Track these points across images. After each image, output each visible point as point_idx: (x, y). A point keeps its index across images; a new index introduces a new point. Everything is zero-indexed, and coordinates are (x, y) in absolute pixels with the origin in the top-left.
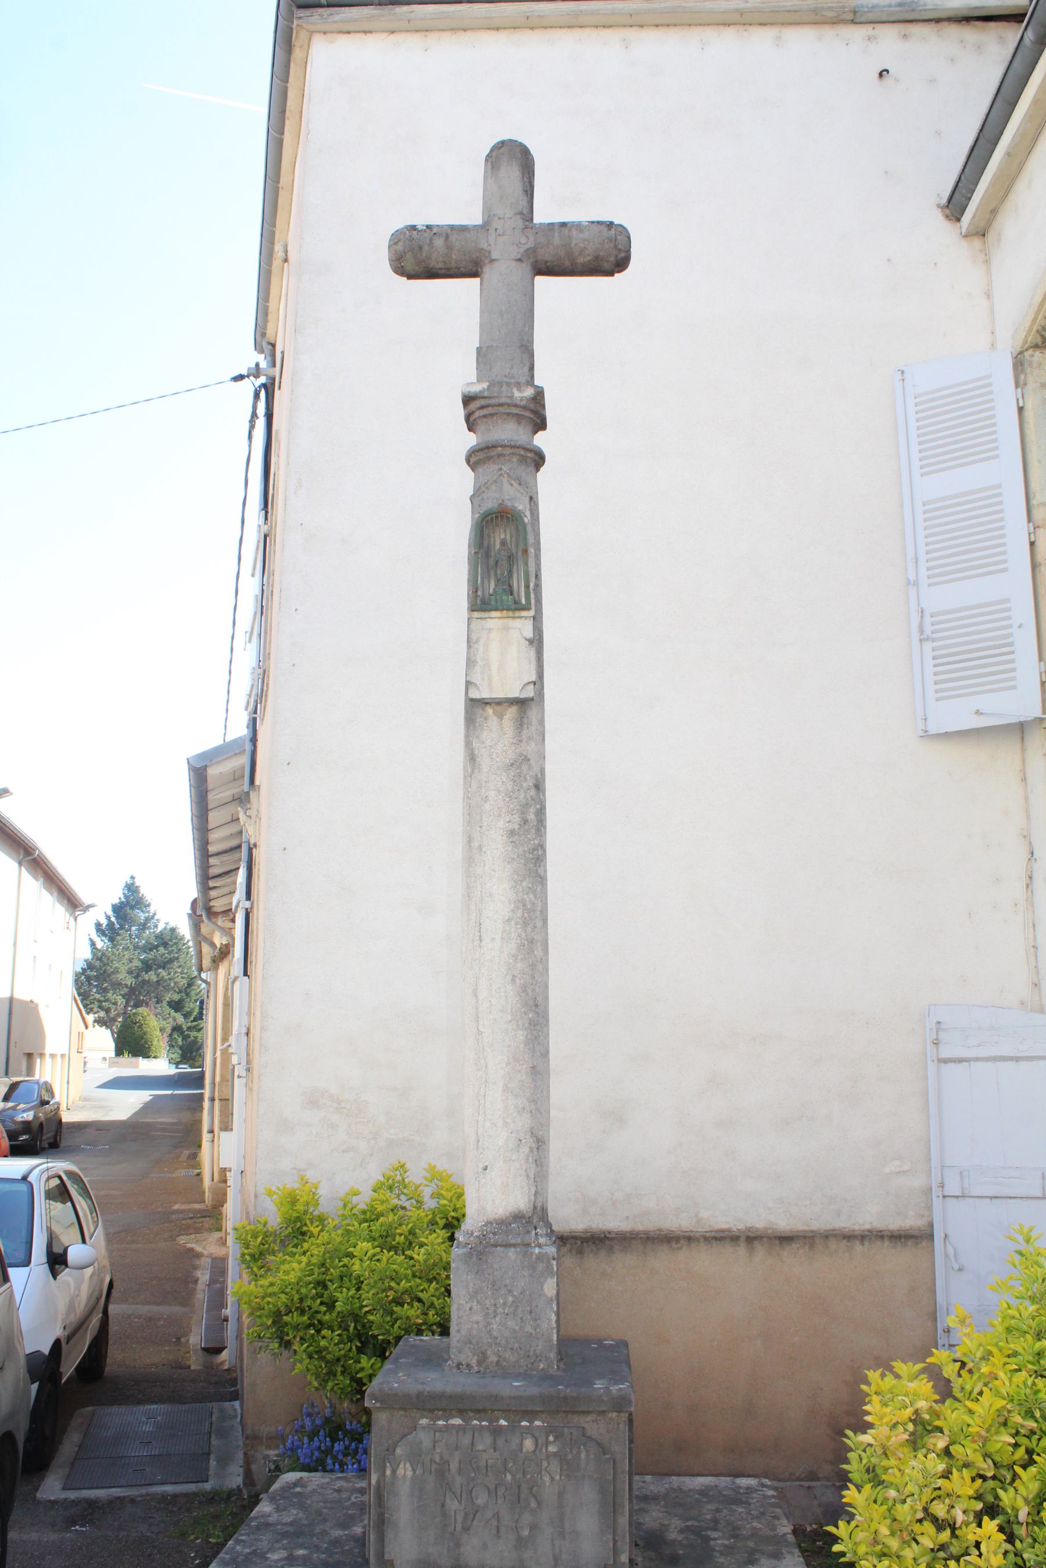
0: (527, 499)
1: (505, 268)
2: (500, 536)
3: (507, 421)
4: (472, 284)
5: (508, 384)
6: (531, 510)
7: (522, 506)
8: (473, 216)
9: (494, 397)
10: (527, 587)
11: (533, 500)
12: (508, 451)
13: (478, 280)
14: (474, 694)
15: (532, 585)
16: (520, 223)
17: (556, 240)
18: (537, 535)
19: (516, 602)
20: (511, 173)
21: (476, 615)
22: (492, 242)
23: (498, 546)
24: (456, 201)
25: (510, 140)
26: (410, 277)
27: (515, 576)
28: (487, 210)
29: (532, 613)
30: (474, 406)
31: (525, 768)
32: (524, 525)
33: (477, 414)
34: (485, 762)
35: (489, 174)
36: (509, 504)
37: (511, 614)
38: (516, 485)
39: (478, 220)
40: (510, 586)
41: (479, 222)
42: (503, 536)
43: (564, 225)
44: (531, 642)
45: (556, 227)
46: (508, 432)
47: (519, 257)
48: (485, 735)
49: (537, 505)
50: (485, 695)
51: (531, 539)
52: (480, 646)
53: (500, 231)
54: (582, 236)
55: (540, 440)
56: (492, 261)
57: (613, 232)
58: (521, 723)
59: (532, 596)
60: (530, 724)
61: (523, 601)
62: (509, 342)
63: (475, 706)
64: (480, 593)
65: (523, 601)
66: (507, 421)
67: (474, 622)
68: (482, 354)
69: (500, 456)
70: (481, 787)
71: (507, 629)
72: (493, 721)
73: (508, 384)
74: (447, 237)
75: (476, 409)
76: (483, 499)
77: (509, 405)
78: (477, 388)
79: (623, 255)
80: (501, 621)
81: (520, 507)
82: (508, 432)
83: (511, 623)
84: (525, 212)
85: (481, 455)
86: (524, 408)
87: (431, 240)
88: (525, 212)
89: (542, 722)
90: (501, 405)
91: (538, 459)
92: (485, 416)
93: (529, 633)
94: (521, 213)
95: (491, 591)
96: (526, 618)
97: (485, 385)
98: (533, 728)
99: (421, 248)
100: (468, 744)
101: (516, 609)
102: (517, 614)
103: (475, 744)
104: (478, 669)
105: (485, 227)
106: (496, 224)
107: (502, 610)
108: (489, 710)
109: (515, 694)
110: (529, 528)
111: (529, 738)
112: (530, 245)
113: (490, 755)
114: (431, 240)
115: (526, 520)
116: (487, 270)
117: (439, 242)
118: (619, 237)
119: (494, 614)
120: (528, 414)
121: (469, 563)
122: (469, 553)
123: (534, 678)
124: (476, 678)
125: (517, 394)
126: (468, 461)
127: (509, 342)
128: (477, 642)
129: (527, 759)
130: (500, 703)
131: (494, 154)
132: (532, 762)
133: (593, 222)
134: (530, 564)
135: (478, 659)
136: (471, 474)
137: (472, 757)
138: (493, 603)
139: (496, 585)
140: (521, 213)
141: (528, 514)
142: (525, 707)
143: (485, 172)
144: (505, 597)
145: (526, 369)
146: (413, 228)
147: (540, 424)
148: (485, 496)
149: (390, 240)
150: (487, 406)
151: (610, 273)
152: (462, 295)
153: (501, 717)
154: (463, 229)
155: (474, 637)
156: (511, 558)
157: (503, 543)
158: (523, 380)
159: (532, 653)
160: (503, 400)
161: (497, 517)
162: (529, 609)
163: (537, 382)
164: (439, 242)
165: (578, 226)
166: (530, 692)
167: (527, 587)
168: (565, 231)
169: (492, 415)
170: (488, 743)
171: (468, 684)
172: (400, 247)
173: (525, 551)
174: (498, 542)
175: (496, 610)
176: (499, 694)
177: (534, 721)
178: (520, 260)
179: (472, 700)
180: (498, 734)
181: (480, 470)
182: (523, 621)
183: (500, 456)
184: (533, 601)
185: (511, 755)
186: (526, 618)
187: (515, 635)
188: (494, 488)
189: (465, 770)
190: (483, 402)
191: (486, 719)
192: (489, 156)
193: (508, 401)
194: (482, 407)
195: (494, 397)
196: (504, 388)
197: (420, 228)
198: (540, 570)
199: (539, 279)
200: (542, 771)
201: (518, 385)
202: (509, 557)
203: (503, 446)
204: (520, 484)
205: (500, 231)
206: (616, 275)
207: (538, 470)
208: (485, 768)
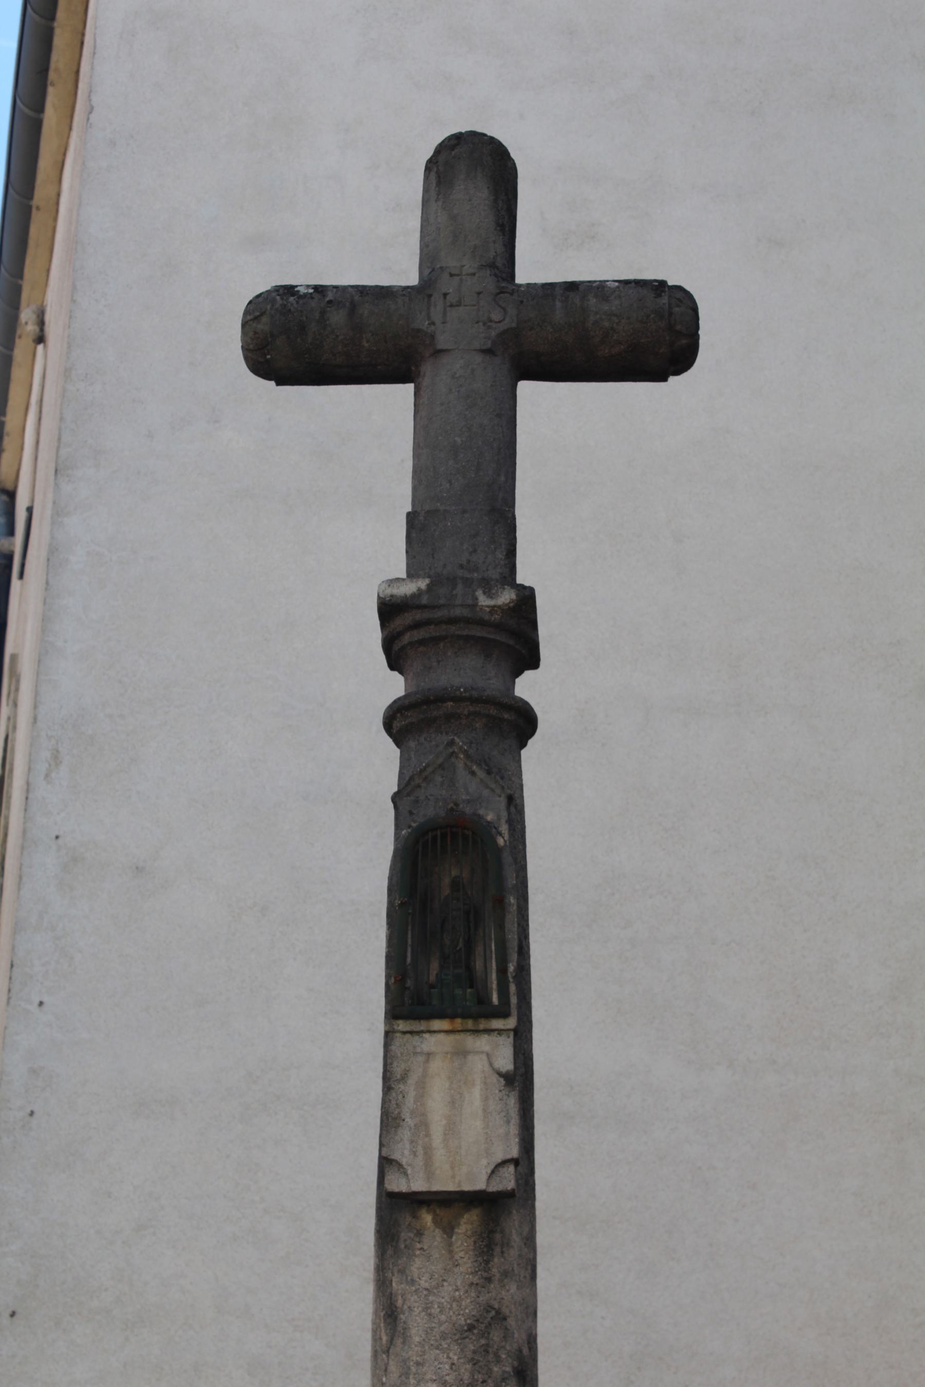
0: (503, 801)
1: (459, 367)
2: (449, 873)
3: (462, 648)
4: (402, 395)
5: (468, 582)
6: (510, 822)
7: (493, 813)
8: (401, 268)
13: (410, 387)
14: (397, 1184)
15: (511, 968)
16: (489, 283)
19: (482, 999)
20: (473, 195)
21: (401, 1025)
23: (446, 891)
24: (374, 242)
25: (473, 134)
27: (479, 949)
28: (429, 258)
29: (511, 1023)
30: (399, 623)
31: (496, 1335)
32: (499, 850)
33: (406, 638)
34: (416, 1324)
35: (433, 193)
36: (468, 810)
37: (470, 1024)
38: (481, 774)
40: (470, 969)
41: (413, 279)
42: (454, 873)
43: (572, 286)
44: (509, 1079)
46: (463, 672)
47: (489, 344)
48: (416, 1266)
49: (521, 812)
50: (419, 1185)
51: (511, 881)
53: (451, 299)
54: (606, 307)
55: (527, 687)
57: (665, 300)
58: (488, 1244)
59: (513, 988)
60: (506, 1244)
61: (495, 999)
62: (466, 505)
63: (398, 1211)
64: (409, 983)
65: (495, 999)
66: (462, 648)
67: (398, 1040)
68: (416, 524)
69: (450, 717)
70: (406, 1374)
71: (462, 1053)
72: (434, 1239)
73: (468, 582)
75: (404, 627)
76: (417, 801)
77: (468, 621)
78: (409, 589)
79: (684, 341)
80: (451, 1038)
81: (489, 818)
82: (463, 672)
83: (470, 1041)
84: (500, 262)
86: (498, 627)
87: (323, 313)
88: (500, 262)
89: (530, 1240)
91: (523, 723)
92: (422, 642)
93: (505, 1060)
94: (492, 266)
95: (432, 978)
96: (500, 1032)
97: (423, 584)
98: (513, 1253)
99: (303, 328)
100: (382, 1284)
101: (476, 1017)
102: (483, 1024)
103: (397, 1285)
104: (405, 1134)
105: (424, 290)
106: (448, 285)
107: (452, 1017)
108: (427, 1218)
109: (480, 1184)
110: (507, 858)
111: (505, 1274)
112: (509, 322)
113: (427, 1309)
114: (323, 313)
115: (501, 842)
116: (427, 369)
117: (337, 318)
118: (676, 310)
119: (437, 1024)
121: (390, 924)
122: (390, 904)
123: (514, 1152)
124: (402, 1152)
125: (484, 601)
126: (389, 724)
127: (466, 505)
128: (404, 1078)
129: (500, 1317)
130: (448, 1203)
131: (442, 158)
132: (511, 1322)
133: (627, 282)
135: (406, 1114)
136: (394, 752)
137: (389, 1313)
138: (435, 1002)
140: (492, 266)
141: (504, 829)
142: (499, 1213)
143: (426, 190)
144: (458, 992)
145: (500, 555)
146: (289, 290)
147: (529, 658)
149: (246, 313)
151: (660, 376)
152: (382, 415)
153: (449, 1230)
154: (382, 293)
155: (398, 1069)
157: (456, 884)
158: (494, 574)
159: (512, 1102)
160: (458, 612)
162: (505, 1015)
163: (523, 577)
164: (337, 318)
165: (598, 289)
166: (507, 1181)
167: (502, 971)
169: (435, 640)
170: (424, 1283)
171: (385, 1163)
172: (264, 326)
173: (500, 903)
174: (447, 881)
175: (441, 1016)
176: (444, 1184)
177: (516, 1240)
179: (392, 1195)
180: (442, 1267)
181: (412, 744)
182: (494, 1038)
183: (450, 717)
184: (514, 1000)
185: (468, 1307)
186: (500, 1032)
187: (478, 1065)
188: (439, 779)
189: (376, 1339)
190: (418, 616)
191: (420, 1234)
192: (431, 165)
193: (466, 612)
194: (416, 626)
197: (302, 290)
198: (526, 937)
199: (526, 389)
200: (532, 1340)
201: (488, 587)
203: (458, 699)
204: (489, 772)
205: (451, 299)
206: (672, 379)
207: (523, 745)
208: (416, 1335)
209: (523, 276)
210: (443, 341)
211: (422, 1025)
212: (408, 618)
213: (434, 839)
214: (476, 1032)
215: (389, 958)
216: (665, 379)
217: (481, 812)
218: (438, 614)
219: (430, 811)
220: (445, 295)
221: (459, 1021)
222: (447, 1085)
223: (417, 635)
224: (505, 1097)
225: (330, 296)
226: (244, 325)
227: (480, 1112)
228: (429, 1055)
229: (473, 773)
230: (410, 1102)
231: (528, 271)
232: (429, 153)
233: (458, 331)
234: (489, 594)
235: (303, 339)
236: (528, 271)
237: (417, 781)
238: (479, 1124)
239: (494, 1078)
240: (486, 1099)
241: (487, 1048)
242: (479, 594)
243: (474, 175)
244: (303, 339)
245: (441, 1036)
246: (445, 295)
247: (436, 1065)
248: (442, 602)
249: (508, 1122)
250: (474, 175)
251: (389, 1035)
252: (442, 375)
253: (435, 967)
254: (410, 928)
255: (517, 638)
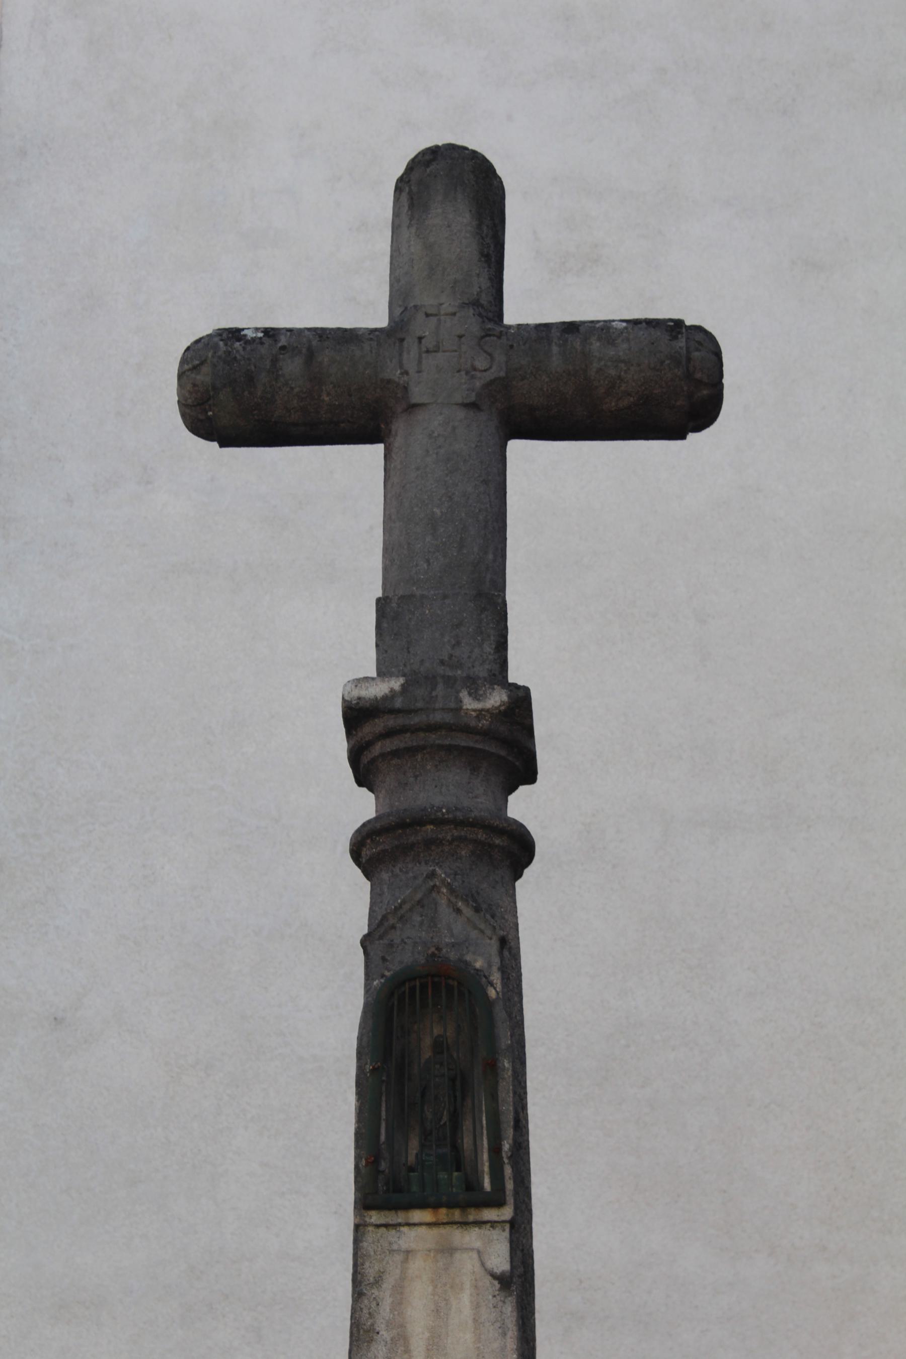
0: (494, 944)
1: (437, 425)
2: (431, 1031)
5: (450, 682)
6: (503, 969)
9: (416, 711)
10: (495, 1150)
11: (508, 948)
12: (449, 833)
13: (378, 449)
15: (506, 1146)
16: (472, 324)
17: (556, 362)
18: (518, 1025)
19: (472, 1185)
20: (453, 219)
21: (375, 1217)
22: (412, 367)
23: (427, 1054)
24: (335, 276)
25: (451, 147)
26: (224, 443)
27: (467, 1125)
28: (400, 294)
29: (507, 1213)
30: (367, 730)
32: (489, 1004)
33: (377, 749)
35: (405, 219)
36: (453, 956)
37: (457, 1214)
38: (468, 912)
39: (377, 317)
40: (456, 1148)
41: (382, 322)
42: (437, 1031)
43: (571, 327)
44: (504, 1281)
45: (555, 333)
46: (445, 789)
47: (473, 398)
49: (516, 956)
51: (505, 1040)
52: (385, 1295)
55: (521, 805)
56: (413, 407)
57: (681, 343)
59: (508, 1171)
61: (487, 1185)
64: (383, 1165)
65: (487, 1185)
67: (371, 1235)
68: (387, 612)
69: (429, 843)
71: (448, 1250)
73: (450, 682)
74: (310, 356)
75: (374, 735)
76: (391, 945)
78: (380, 689)
79: (705, 392)
80: (435, 1231)
81: (478, 965)
82: (445, 789)
83: (458, 1236)
84: (484, 300)
85: (386, 843)
86: (485, 734)
87: (275, 361)
88: (484, 300)
90: (431, 728)
91: (518, 849)
92: (396, 753)
93: (499, 1258)
94: (476, 303)
95: (412, 1159)
96: (493, 1224)
97: (396, 684)
99: (251, 379)
101: (465, 1206)
105: (395, 333)
106: (422, 327)
107: (435, 1206)
110: (500, 1013)
114: (275, 361)
115: (492, 993)
116: (399, 426)
117: (292, 367)
118: (696, 354)
119: (418, 1215)
120: (492, 748)
121: (360, 1094)
122: (360, 1069)
125: (469, 704)
126: (356, 853)
128: (378, 1282)
131: (415, 176)
133: (636, 322)
134: (502, 1095)
135: (381, 1326)
138: (415, 1188)
139: (422, 1146)
140: (476, 303)
141: (496, 977)
143: (396, 214)
144: (443, 1176)
145: (489, 648)
146: (235, 334)
148: (396, 936)
149: (184, 361)
150: (403, 730)
152: (346, 481)
154: (345, 338)
155: (370, 1270)
156: (460, 1085)
157: (439, 1046)
158: (481, 671)
159: (509, 1310)
160: (438, 717)
161: (423, 987)
162: (497, 1202)
164: (292, 367)
165: (602, 330)
167: (495, 1150)
168: (576, 342)
169: (411, 751)
172: (204, 377)
173: (492, 1066)
174: (427, 1042)
178: (473, 406)
181: (385, 876)
182: (486, 1231)
183: (429, 843)
184: (510, 1185)
186: (493, 1224)
187: (467, 1264)
188: (417, 918)
190: (391, 722)
192: (402, 184)
193: (448, 718)
194: (389, 734)
195: (416, 711)
196: (440, 687)
197: (250, 334)
199: (516, 448)
201: (474, 686)
202: (453, 1080)
203: (440, 822)
204: (477, 910)
205: (429, 343)
206: (691, 436)
207: (518, 875)
209: (513, 315)
210: (418, 394)
211: (400, 1217)
212: (379, 725)
213: (412, 990)
214: (464, 1224)
215: (358, 1135)
216: (683, 437)
217: (468, 958)
218: (415, 720)
219: (407, 957)
220: (420, 339)
221: (443, 1211)
222: (430, 1289)
223: (390, 745)
224: (500, 1304)
225: (283, 341)
226: (181, 376)
227: (470, 1322)
228: (408, 1252)
229: (458, 911)
230: (385, 1310)
231: (518, 310)
232: (400, 170)
233: (436, 381)
234: (476, 695)
235: (250, 392)
236: (518, 310)
237: (392, 921)
238: (469, 1337)
239: (488, 1280)
240: (477, 1306)
241: (478, 1244)
242: (465, 696)
243: (454, 196)
244: (250, 392)
245: (423, 1230)
246: (420, 339)
247: (417, 1265)
248: (420, 705)
249: (504, 1334)
250: (454, 196)
251: (359, 1229)
252: (416, 434)
253: (414, 1144)
254: (384, 1099)
255: (509, 747)
